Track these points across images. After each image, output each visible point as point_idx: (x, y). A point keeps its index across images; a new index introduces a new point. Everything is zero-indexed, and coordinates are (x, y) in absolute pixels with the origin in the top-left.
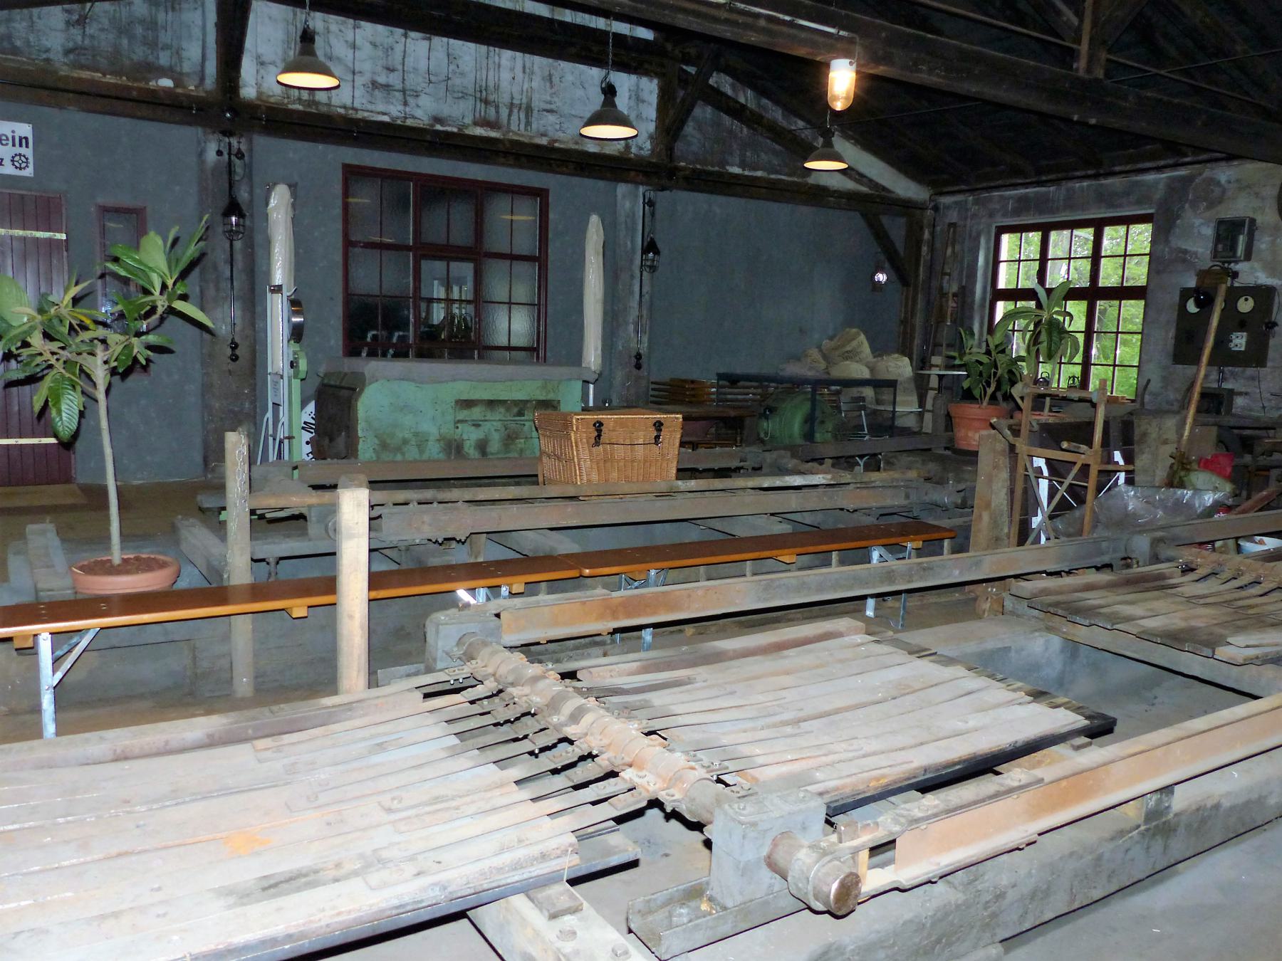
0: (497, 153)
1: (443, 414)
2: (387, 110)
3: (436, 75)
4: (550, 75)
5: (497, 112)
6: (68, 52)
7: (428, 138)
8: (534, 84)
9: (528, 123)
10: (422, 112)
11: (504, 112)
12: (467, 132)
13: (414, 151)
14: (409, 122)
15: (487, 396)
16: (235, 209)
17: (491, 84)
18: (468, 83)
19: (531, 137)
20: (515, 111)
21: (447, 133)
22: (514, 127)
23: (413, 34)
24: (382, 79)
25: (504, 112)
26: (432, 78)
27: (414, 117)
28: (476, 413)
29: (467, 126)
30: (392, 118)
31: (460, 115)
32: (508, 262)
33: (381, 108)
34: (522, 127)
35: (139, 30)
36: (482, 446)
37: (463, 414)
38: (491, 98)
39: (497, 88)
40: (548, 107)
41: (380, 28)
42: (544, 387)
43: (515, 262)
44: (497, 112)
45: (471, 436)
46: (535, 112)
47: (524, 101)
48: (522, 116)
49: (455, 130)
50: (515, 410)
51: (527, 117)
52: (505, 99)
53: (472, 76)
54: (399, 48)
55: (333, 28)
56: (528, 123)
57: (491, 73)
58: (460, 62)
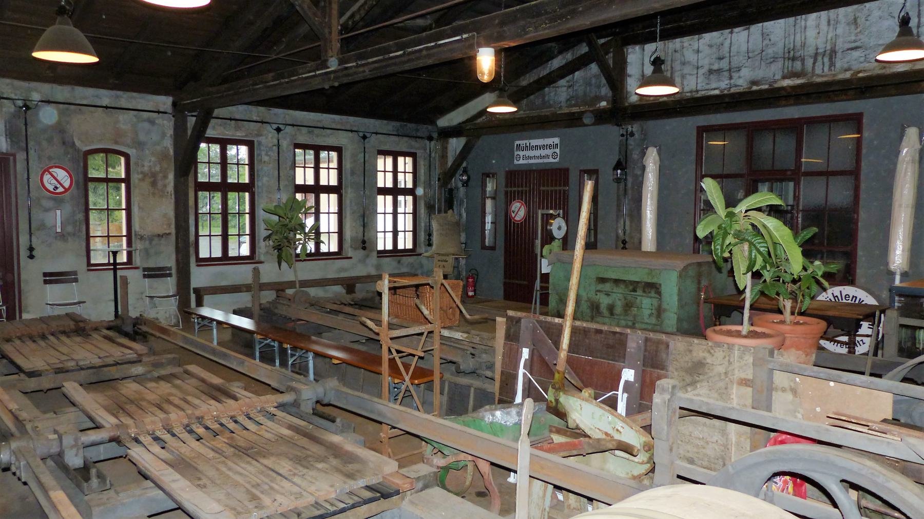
0: (779, 98)
1: (590, 285)
2: (718, 86)
3: (753, 52)
4: (855, 19)
5: (803, 64)
6: (568, 100)
7: (727, 100)
8: (840, 31)
9: (832, 64)
10: (741, 82)
11: (809, 62)
12: (776, 86)
13: (717, 111)
14: (733, 90)
15: (614, 276)
16: (626, 166)
17: (798, 44)
18: (779, 49)
19: (834, 75)
20: (820, 58)
21: (760, 91)
22: (818, 71)
23: (736, 30)
24: (715, 67)
25: (809, 62)
26: (750, 55)
27: (736, 86)
28: (608, 287)
29: (775, 82)
30: (721, 91)
31: (773, 75)
32: (824, 178)
33: (714, 85)
34: (826, 69)
35: (593, 81)
36: (611, 308)
37: (600, 287)
38: (798, 54)
39: (804, 45)
40: (853, 45)
41: (715, 34)
42: (649, 274)
43: (831, 178)
44: (803, 64)
45: (604, 301)
46: (839, 55)
47: (829, 47)
48: (826, 60)
49: (766, 87)
50: (631, 288)
51: (831, 59)
52: (811, 51)
53: (781, 45)
54: (728, 41)
55: (686, 44)
56: (832, 64)
57: (798, 35)
58: (772, 37)
